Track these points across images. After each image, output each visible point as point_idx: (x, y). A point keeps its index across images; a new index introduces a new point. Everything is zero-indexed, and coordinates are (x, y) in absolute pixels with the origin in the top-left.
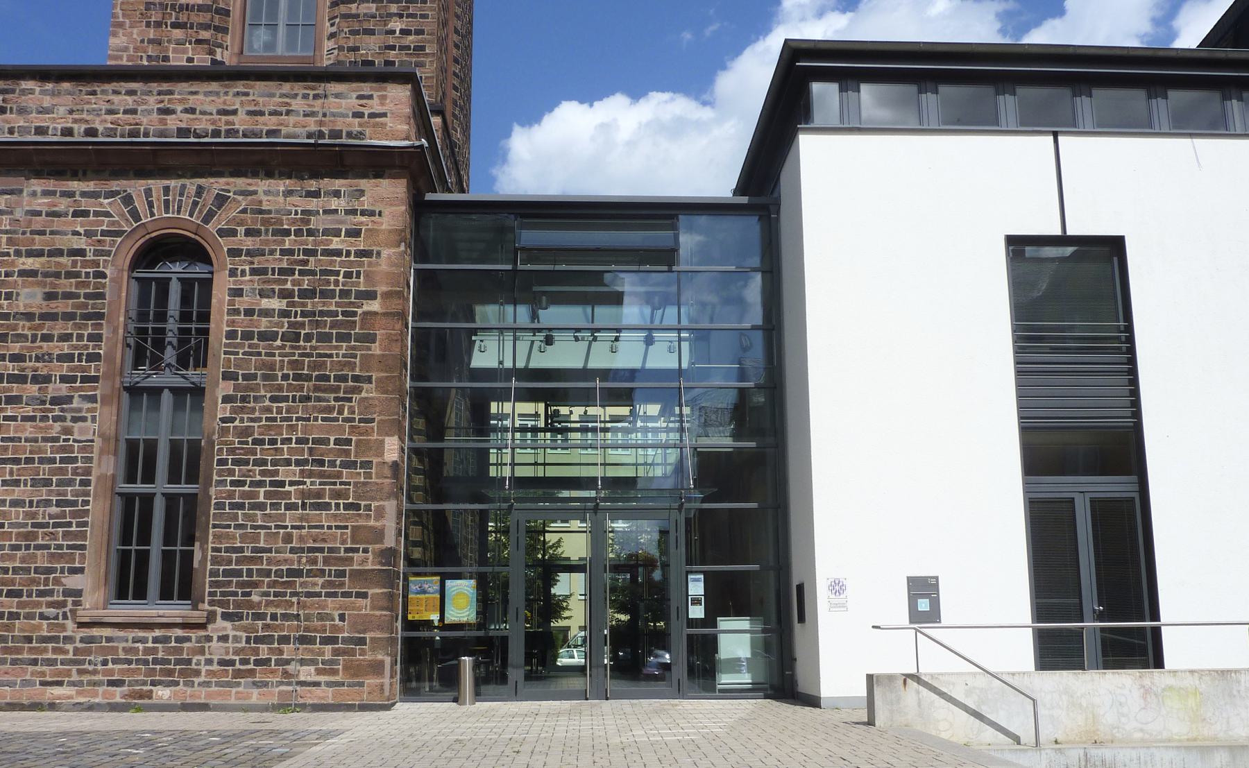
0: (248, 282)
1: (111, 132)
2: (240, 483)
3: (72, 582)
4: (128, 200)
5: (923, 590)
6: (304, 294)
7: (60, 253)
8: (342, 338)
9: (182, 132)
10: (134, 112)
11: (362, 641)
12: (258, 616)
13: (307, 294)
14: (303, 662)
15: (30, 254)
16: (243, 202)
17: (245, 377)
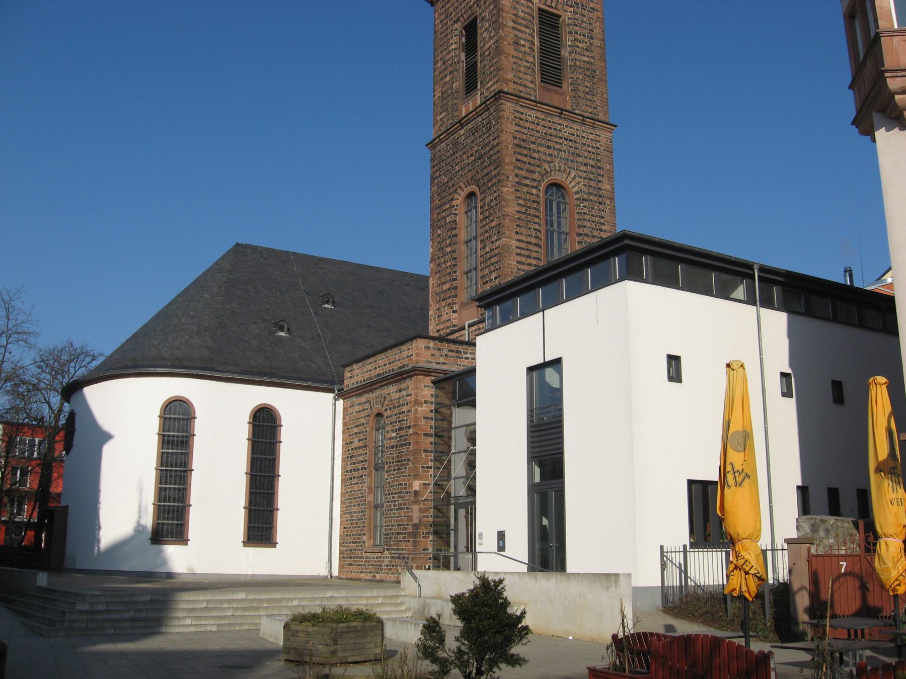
3: (365, 538)
5: (501, 536)
6: (401, 429)
9: (378, 375)
13: (401, 429)
15: (357, 426)
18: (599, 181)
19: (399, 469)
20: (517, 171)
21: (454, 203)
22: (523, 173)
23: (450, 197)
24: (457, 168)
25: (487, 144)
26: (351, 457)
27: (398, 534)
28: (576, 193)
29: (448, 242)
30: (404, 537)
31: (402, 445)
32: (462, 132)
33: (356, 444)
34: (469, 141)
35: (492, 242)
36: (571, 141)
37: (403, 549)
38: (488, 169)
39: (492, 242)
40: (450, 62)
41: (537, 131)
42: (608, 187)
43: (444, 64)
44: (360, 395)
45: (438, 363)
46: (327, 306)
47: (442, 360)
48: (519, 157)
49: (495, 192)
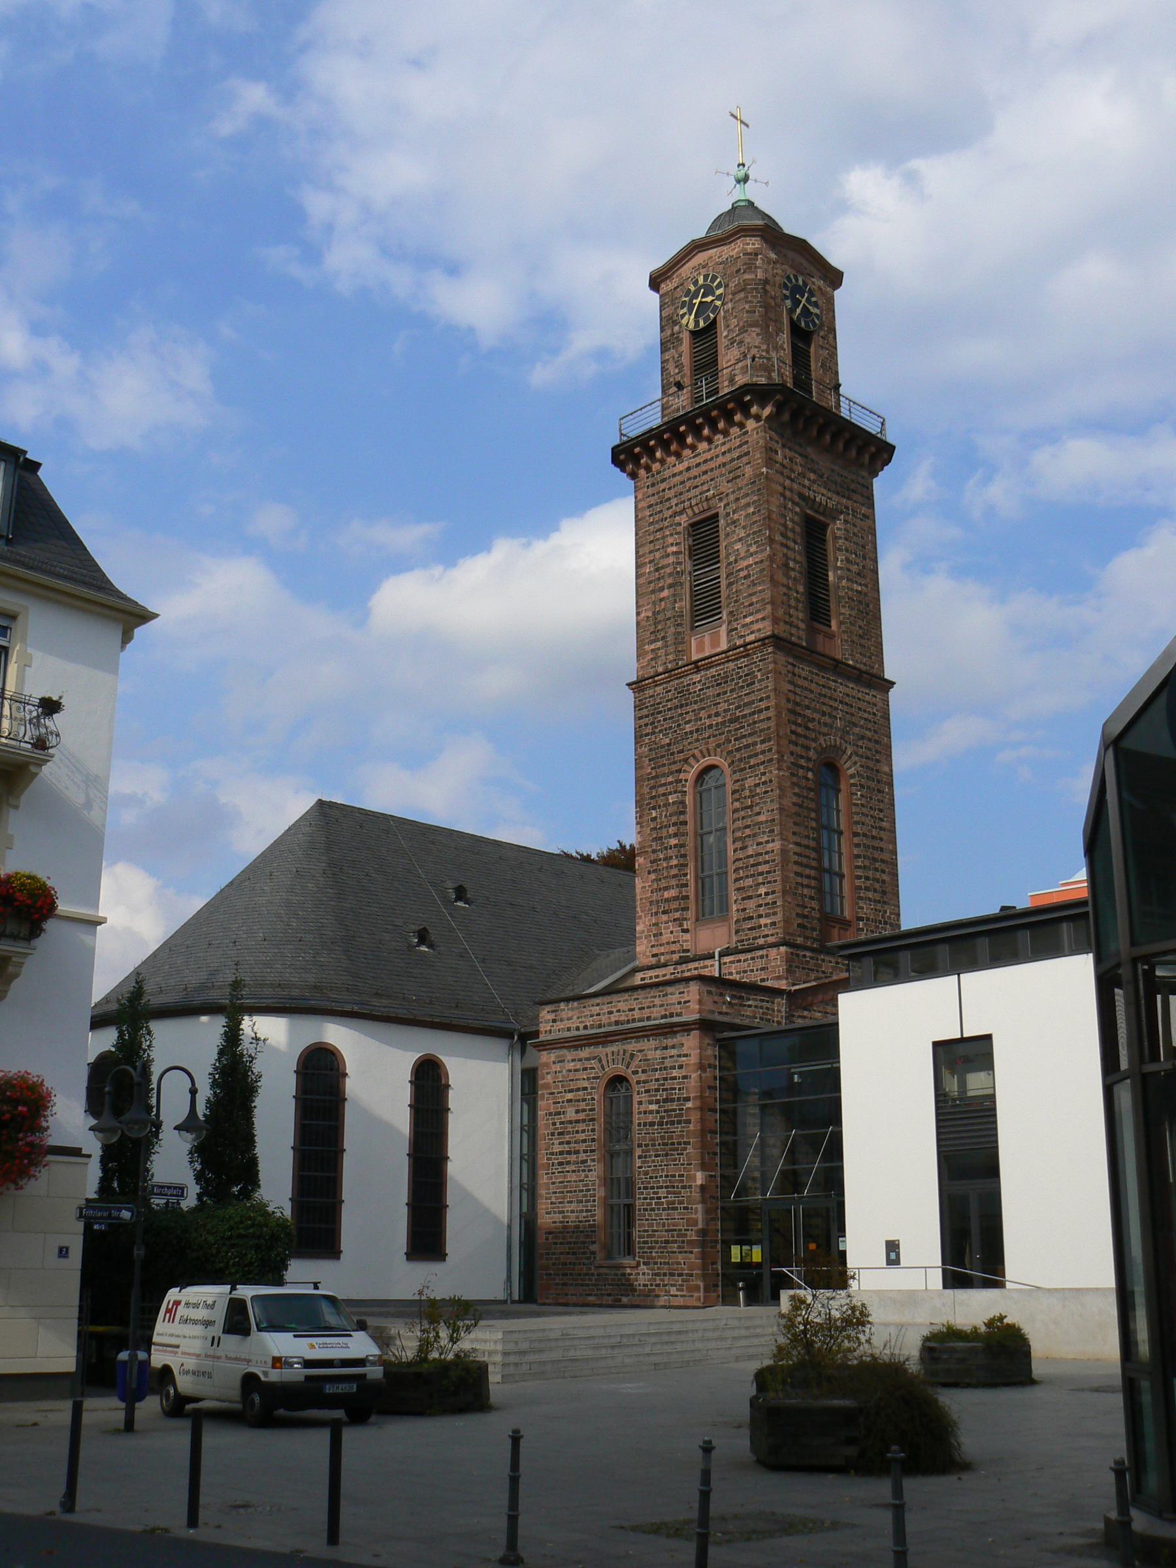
0: (644, 1097)
1: (592, 1026)
2: (645, 1199)
3: (594, 1248)
4: (600, 1061)
5: (892, 1247)
6: (666, 1101)
7: (578, 1090)
8: (679, 1122)
9: (617, 1023)
10: (598, 1015)
11: (691, 1275)
12: (656, 1263)
13: (666, 1101)
14: (672, 1285)
15: (571, 1091)
16: (640, 1056)
17: (646, 1145)
18: (878, 761)
19: (667, 1155)
20: (792, 748)
21: (682, 776)
22: (799, 750)
23: (674, 768)
24: (688, 728)
25: (746, 705)
26: (559, 1134)
27: (667, 1242)
28: (852, 776)
29: (672, 830)
30: (679, 1247)
31: (672, 1123)
32: (697, 677)
33: (571, 1114)
34: (710, 692)
35: (759, 844)
36: (847, 704)
37: (679, 1263)
38: (750, 740)
39: (759, 844)
40: (668, 570)
41: (812, 692)
42: (886, 769)
43: (657, 570)
44: (576, 1047)
45: (720, 1013)
46: (460, 904)
47: (724, 1009)
48: (794, 727)
49: (764, 774)
